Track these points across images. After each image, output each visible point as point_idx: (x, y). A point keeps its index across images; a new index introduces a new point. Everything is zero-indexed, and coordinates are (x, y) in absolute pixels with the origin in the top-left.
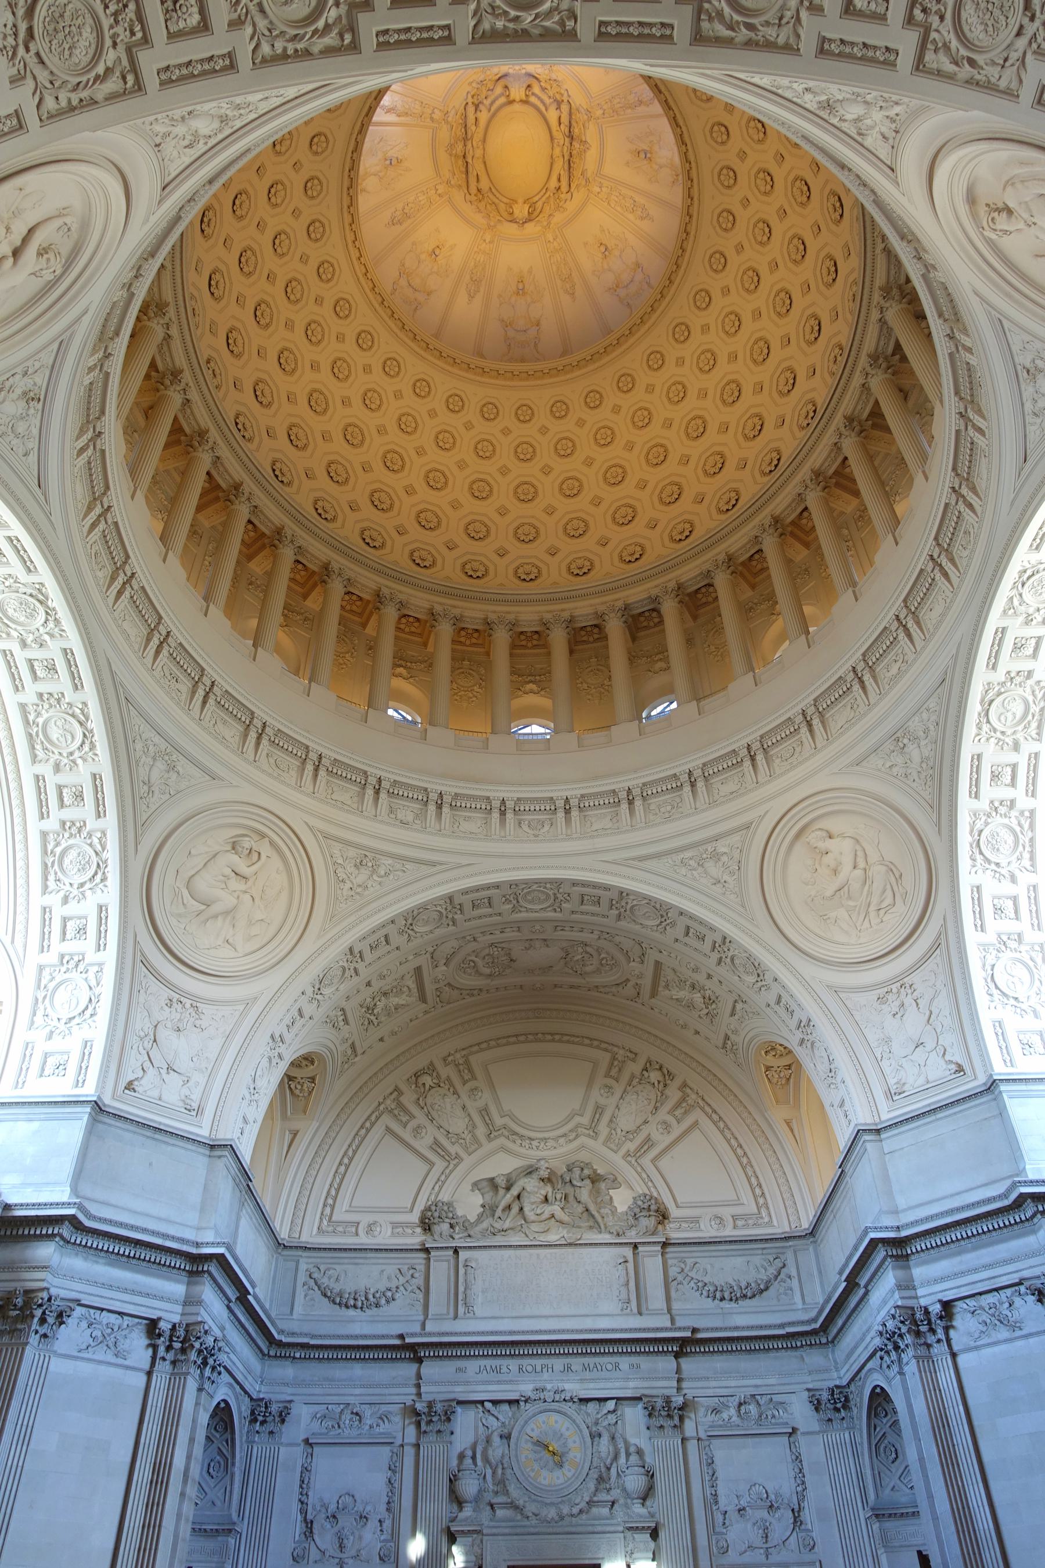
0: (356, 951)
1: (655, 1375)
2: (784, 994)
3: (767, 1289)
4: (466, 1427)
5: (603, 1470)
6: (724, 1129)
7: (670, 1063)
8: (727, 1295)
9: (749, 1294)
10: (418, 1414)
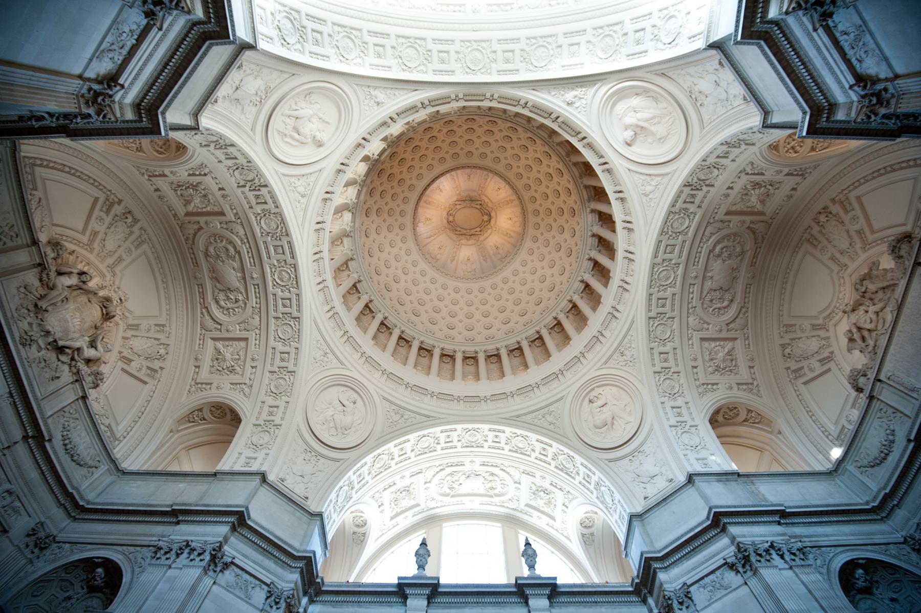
2: (281, 409)
3: (81, 466)
9: (75, 458)
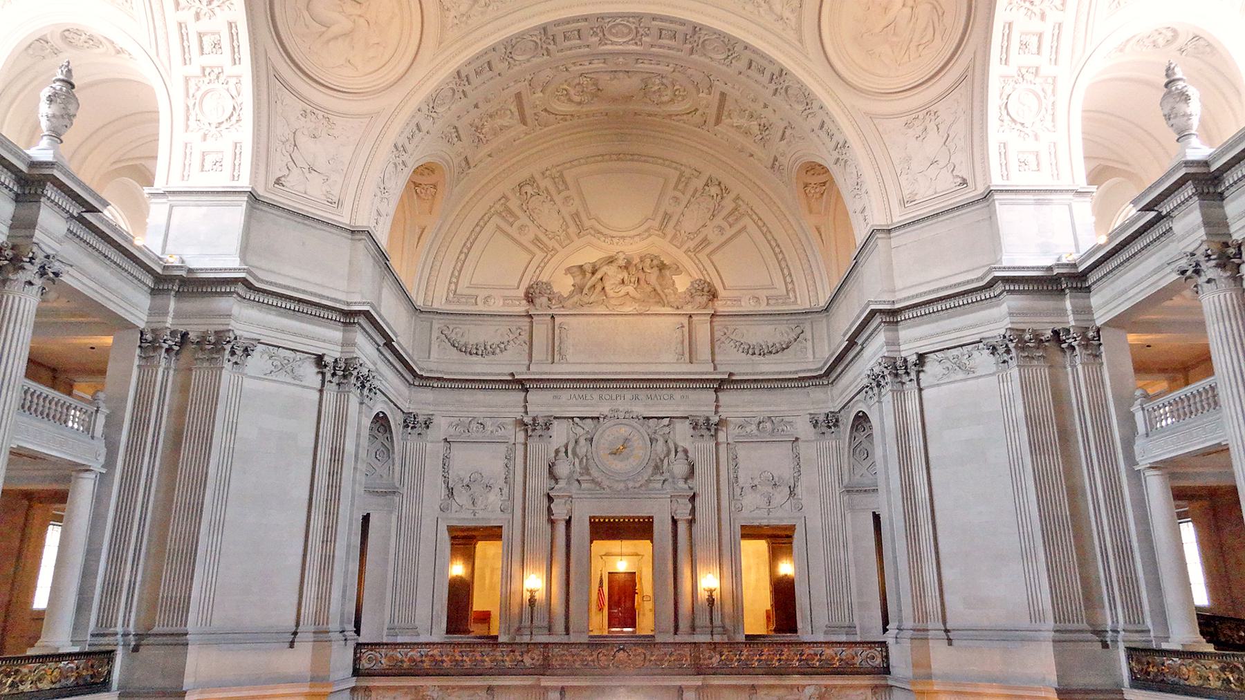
0: (463, 75)
1: (701, 403)
2: (826, 119)
4: (560, 434)
6: (766, 232)
7: (727, 181)
8: (757, 352)
10: (526, 425)
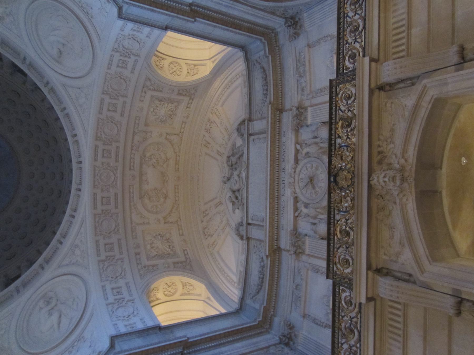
5: (320, 151)
8: (266, 88)
